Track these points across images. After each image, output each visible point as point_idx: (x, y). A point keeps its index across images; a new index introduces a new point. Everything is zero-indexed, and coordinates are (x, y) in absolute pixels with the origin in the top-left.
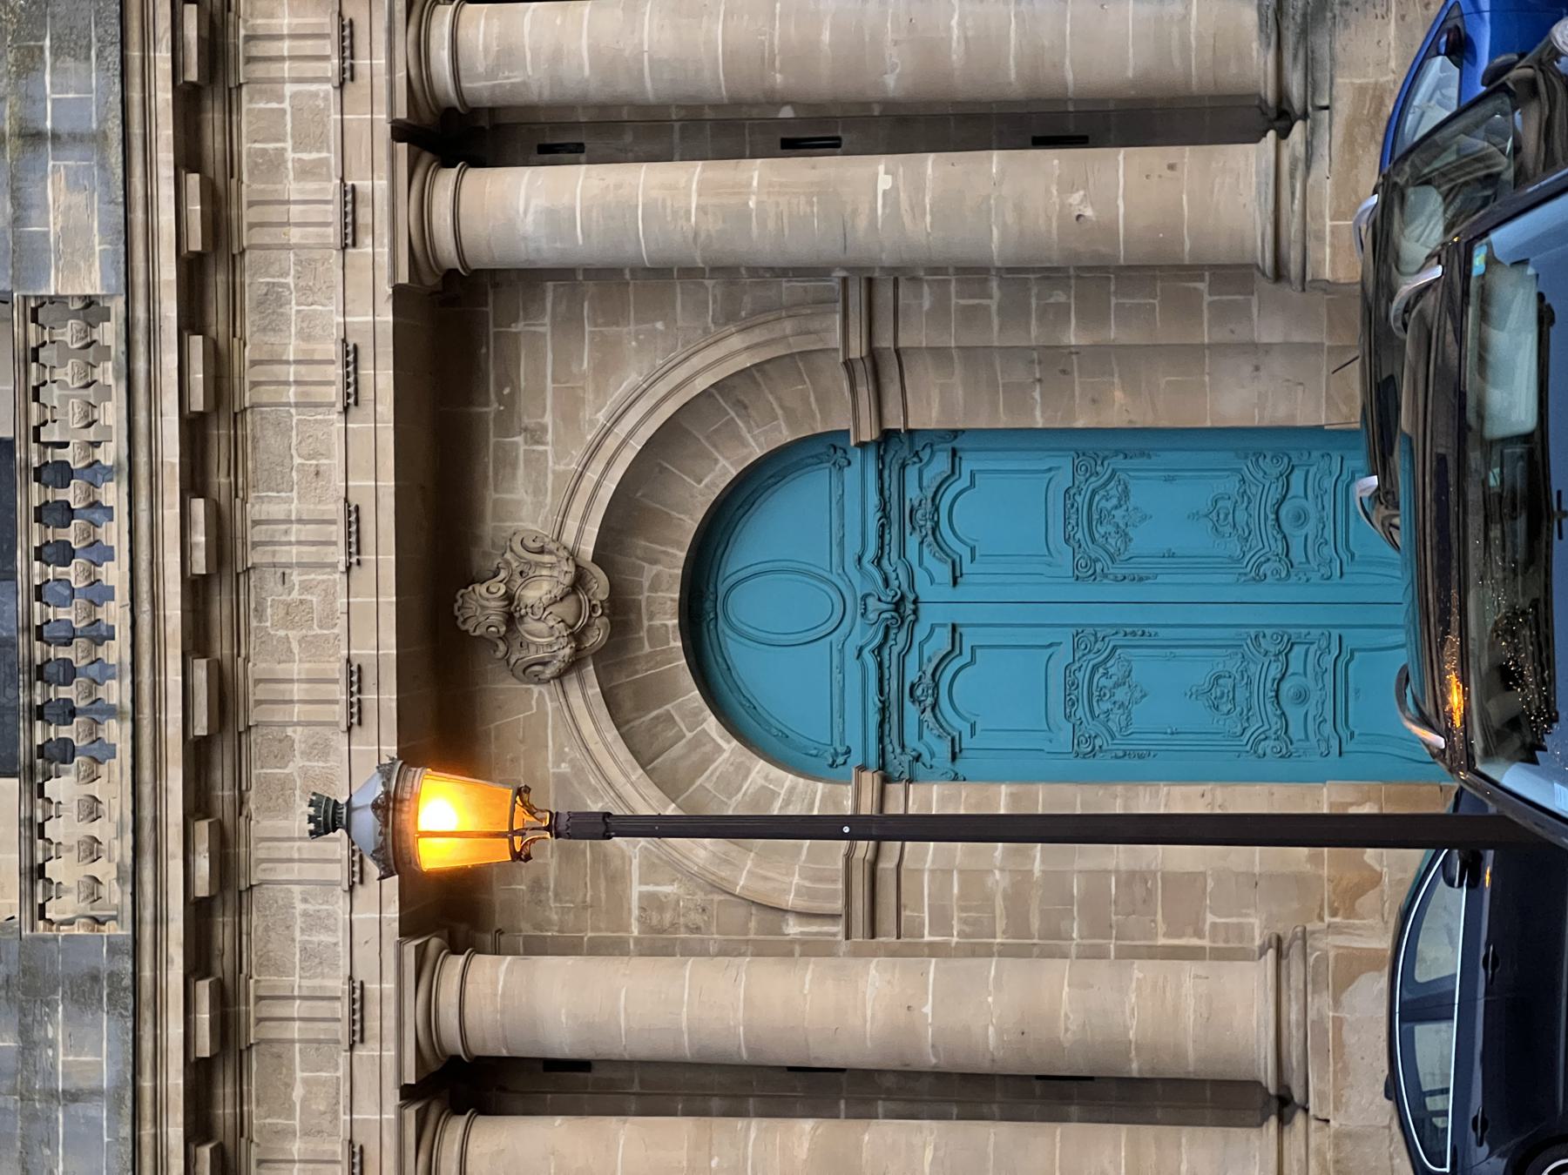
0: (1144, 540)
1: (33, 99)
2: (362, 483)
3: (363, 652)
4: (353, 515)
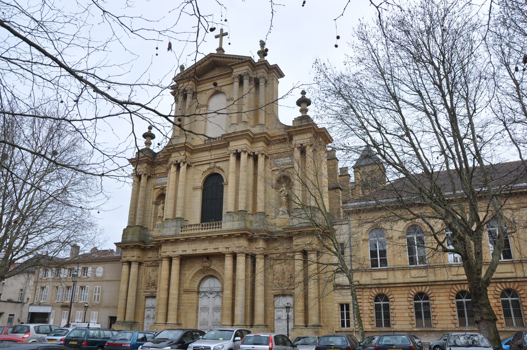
0: (215, 313)
1: (236, 222)
2: (209, 250)
3: (197, 251)
4: (206, 249)
